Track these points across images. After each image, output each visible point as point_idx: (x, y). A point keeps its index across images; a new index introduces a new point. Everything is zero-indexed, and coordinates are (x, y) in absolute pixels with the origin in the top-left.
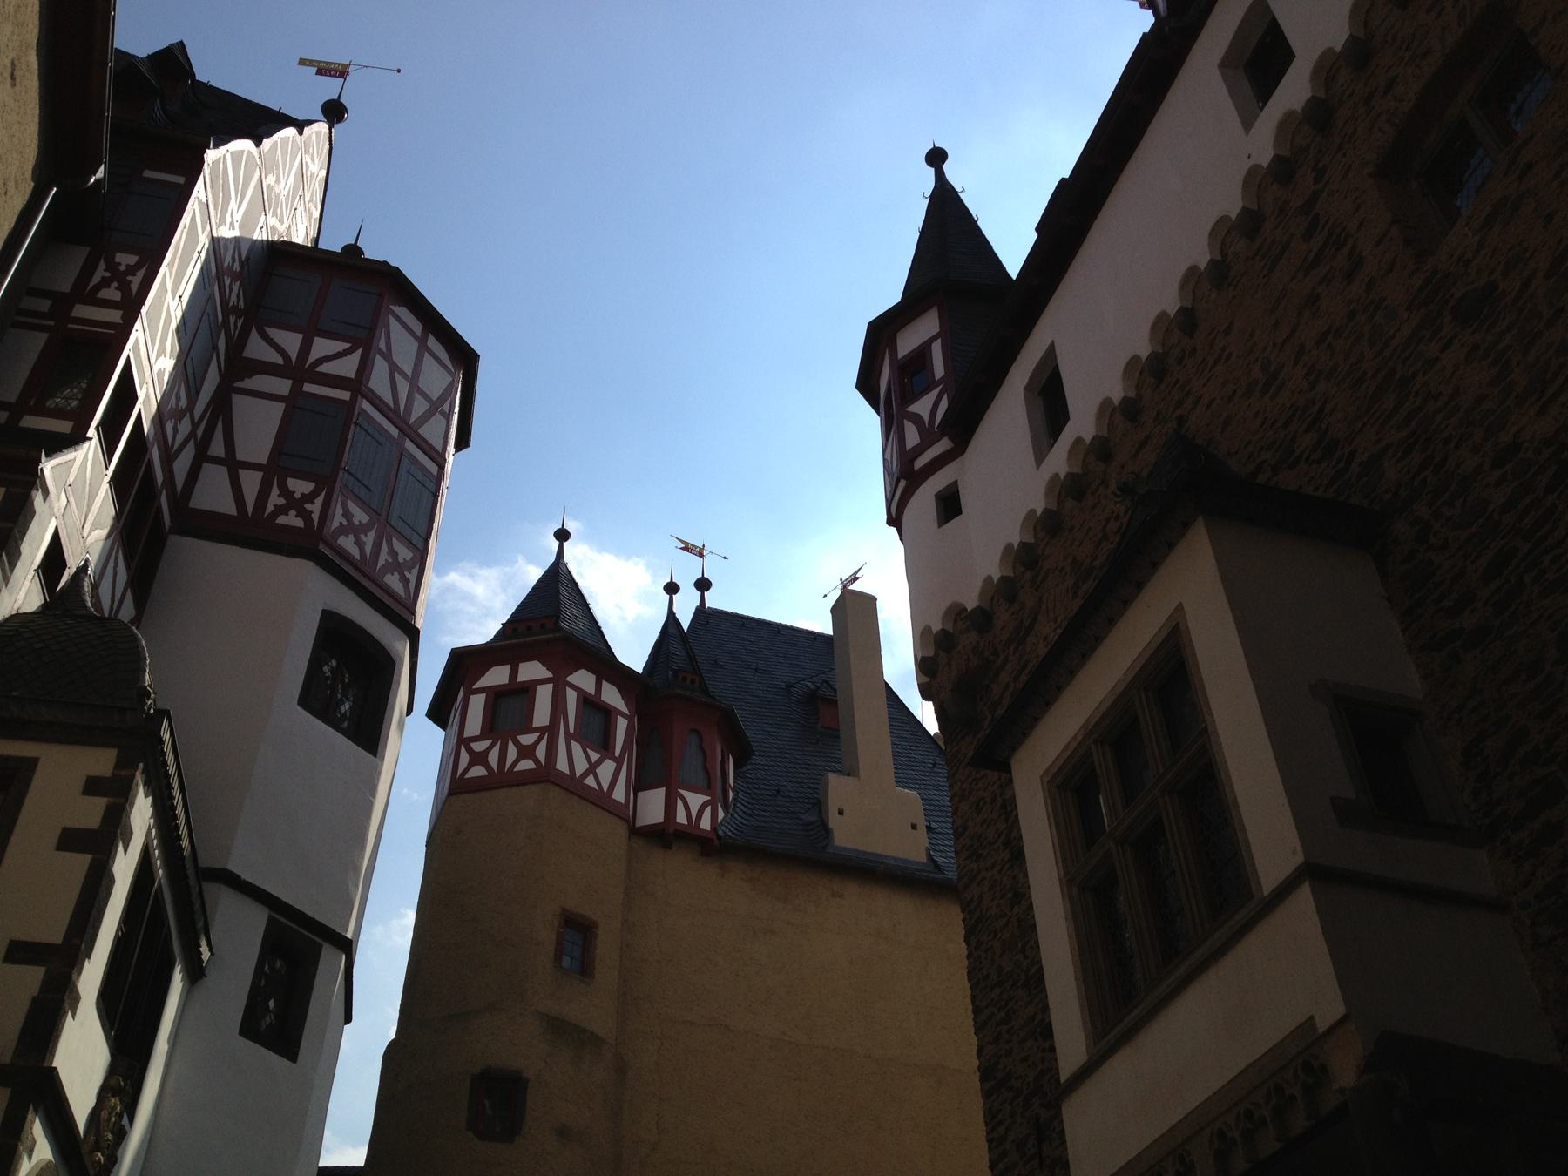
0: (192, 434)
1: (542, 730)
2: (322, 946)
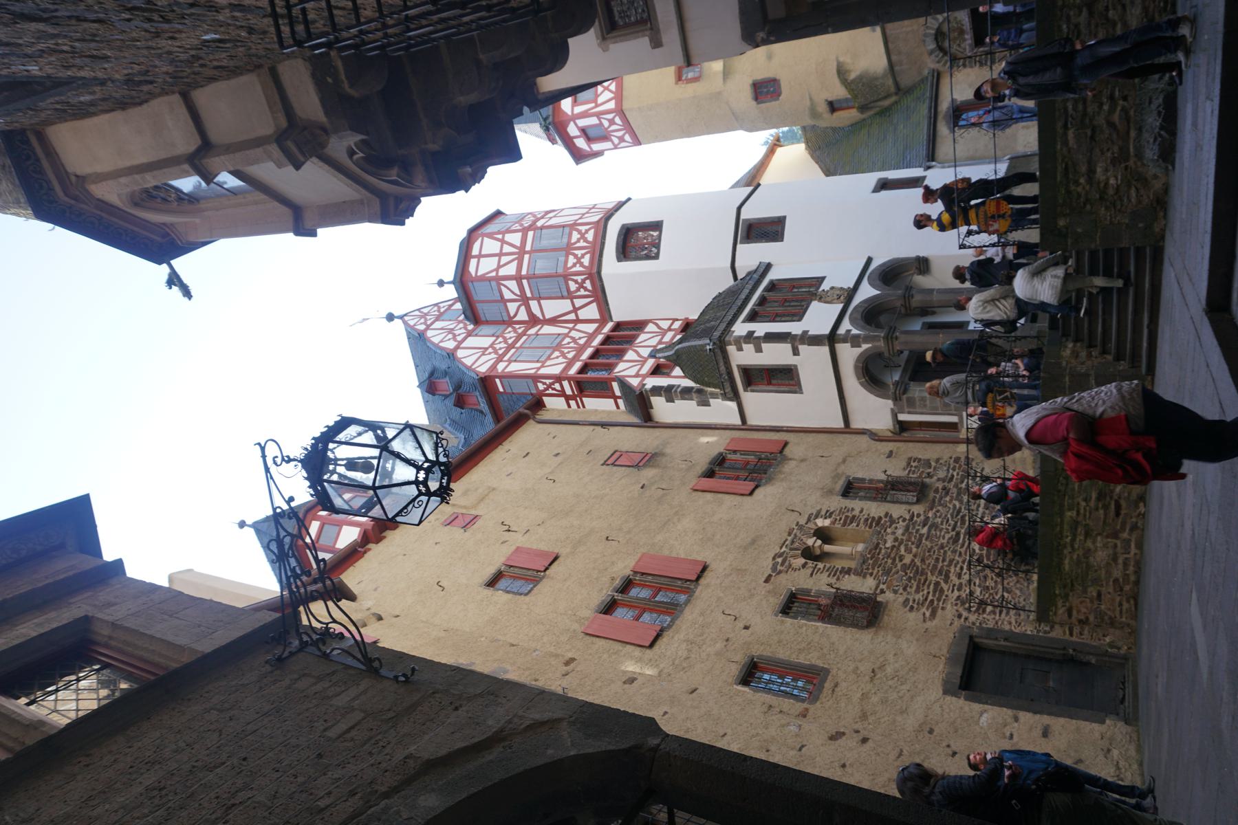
1: (599, 119)
2: (743, 220)
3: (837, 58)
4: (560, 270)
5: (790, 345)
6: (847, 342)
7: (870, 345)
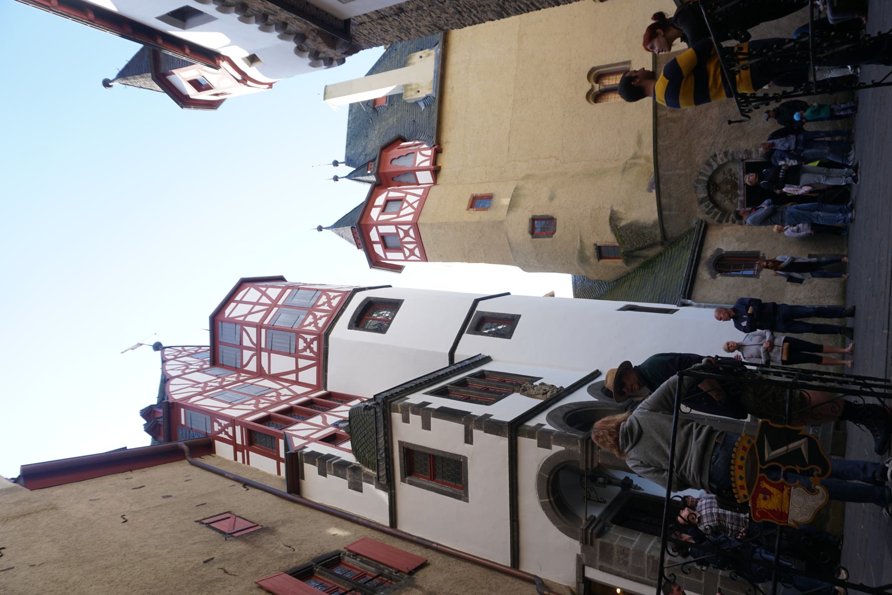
0: (287, 388)
1: (397, 228)
2: (477, 311)
3: (612, 207)
4: (296, 327)
5: (463, 426)
6: (534, 438)
7: (563, 448)
